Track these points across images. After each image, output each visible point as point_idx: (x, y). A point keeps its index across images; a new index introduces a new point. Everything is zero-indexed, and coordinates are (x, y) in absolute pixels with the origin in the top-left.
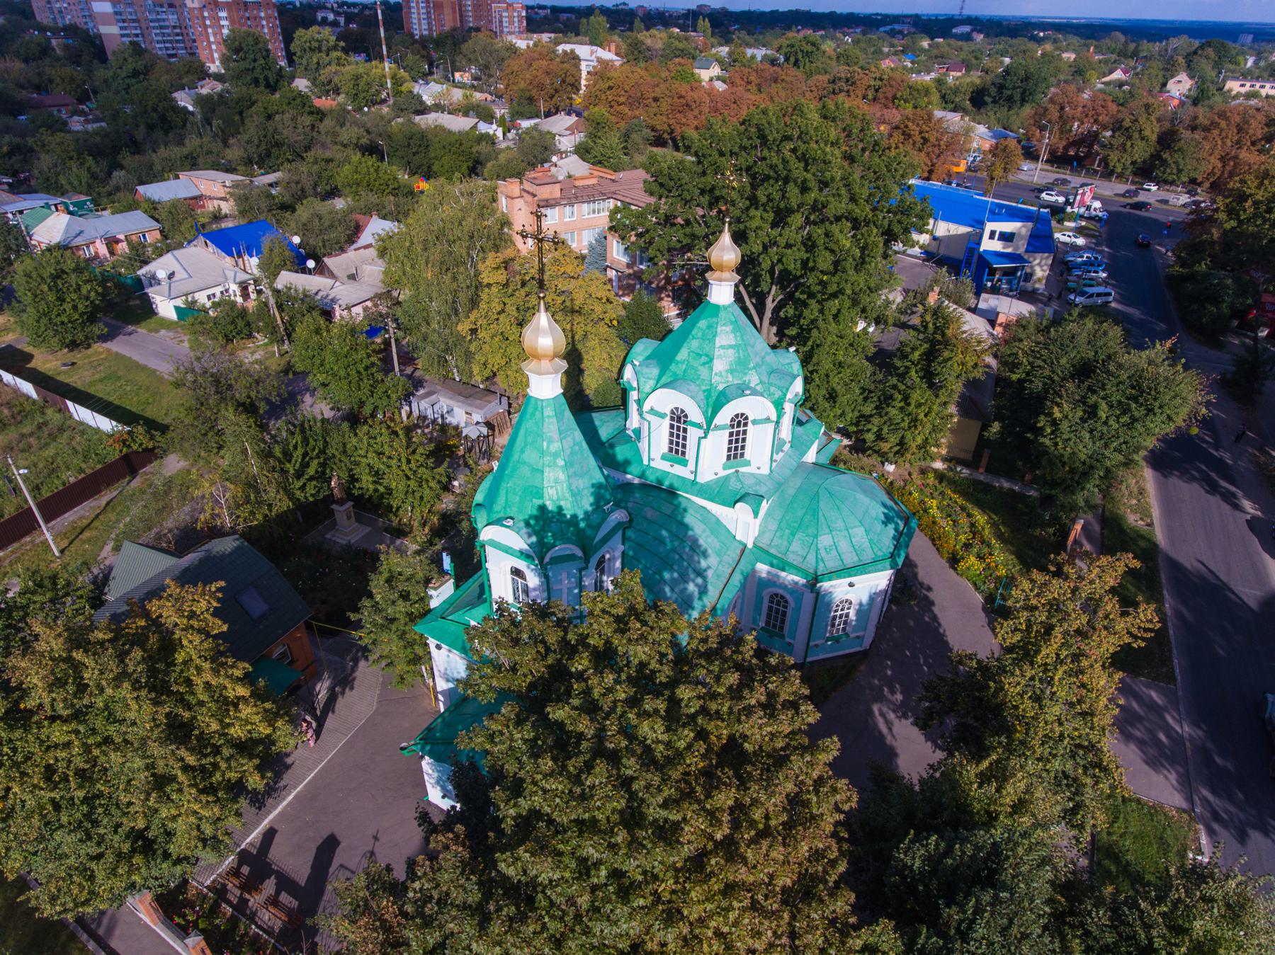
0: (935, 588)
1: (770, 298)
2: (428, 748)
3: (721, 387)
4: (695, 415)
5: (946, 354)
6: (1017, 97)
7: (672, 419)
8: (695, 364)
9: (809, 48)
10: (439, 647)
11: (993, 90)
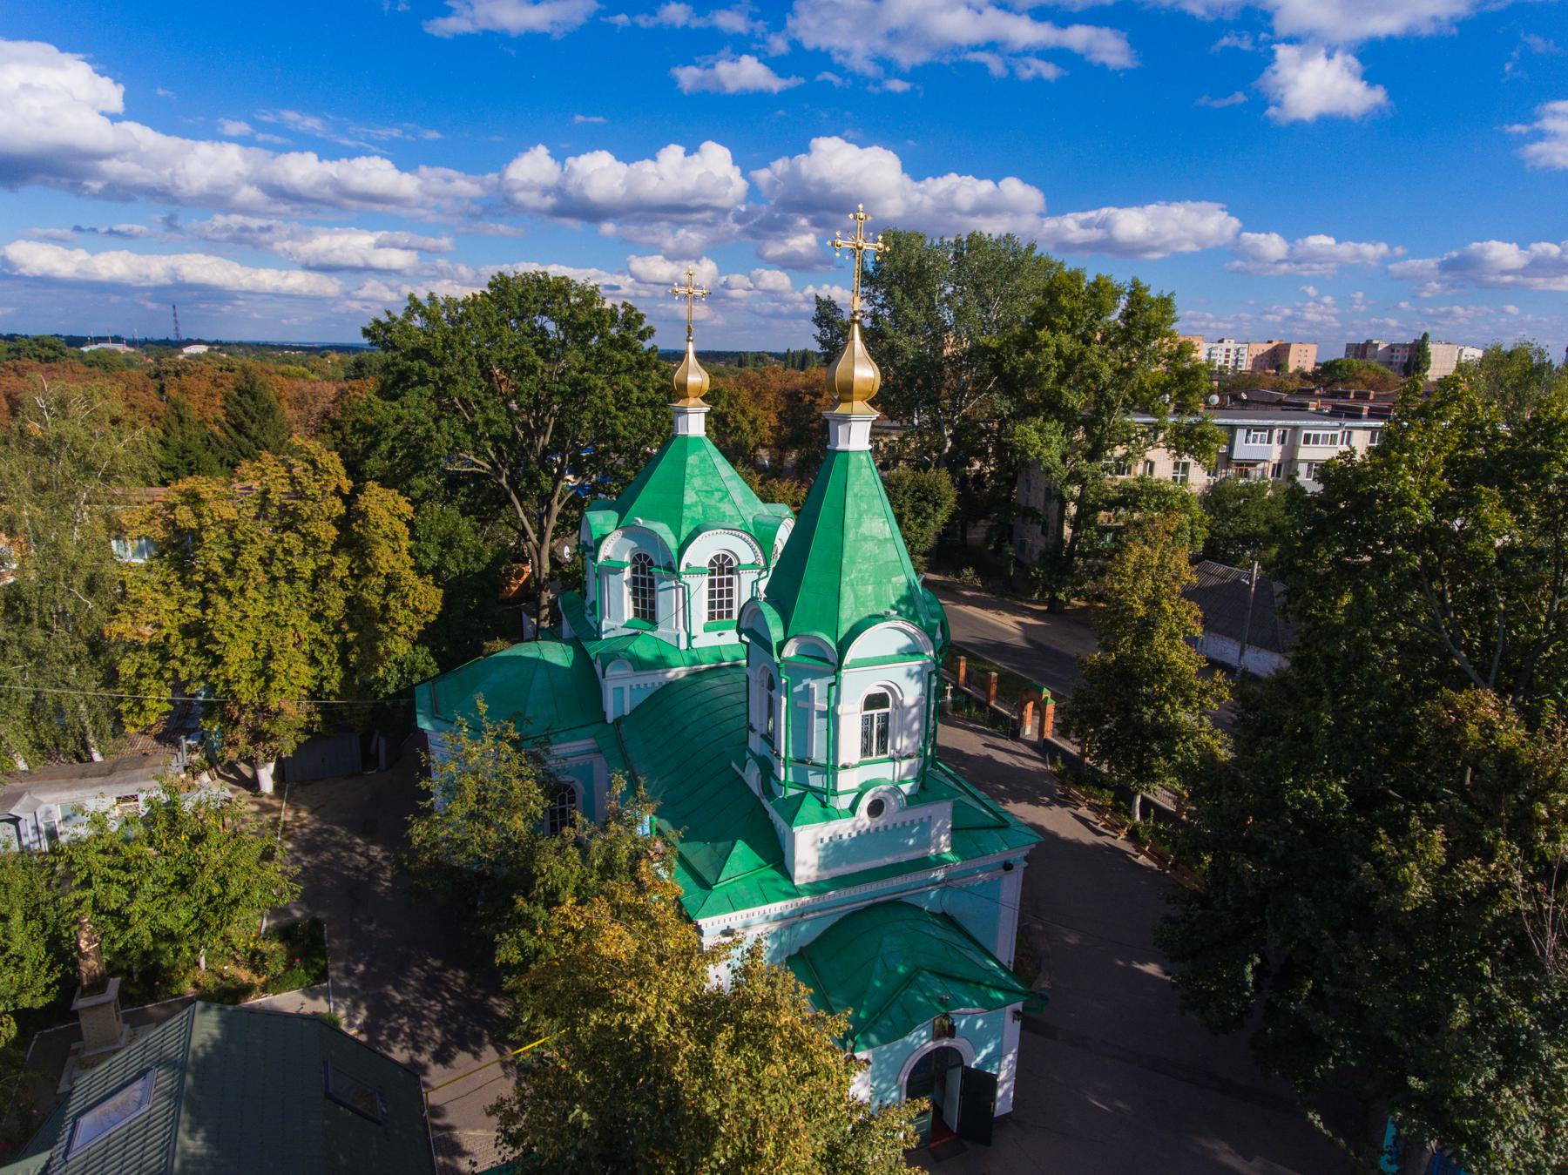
1: (556, 498)
2: (873, 1038)
3: (751, 520)
4: (746, 553)
7: (713, 573)
8: (712, 502)
9: (51, 353)
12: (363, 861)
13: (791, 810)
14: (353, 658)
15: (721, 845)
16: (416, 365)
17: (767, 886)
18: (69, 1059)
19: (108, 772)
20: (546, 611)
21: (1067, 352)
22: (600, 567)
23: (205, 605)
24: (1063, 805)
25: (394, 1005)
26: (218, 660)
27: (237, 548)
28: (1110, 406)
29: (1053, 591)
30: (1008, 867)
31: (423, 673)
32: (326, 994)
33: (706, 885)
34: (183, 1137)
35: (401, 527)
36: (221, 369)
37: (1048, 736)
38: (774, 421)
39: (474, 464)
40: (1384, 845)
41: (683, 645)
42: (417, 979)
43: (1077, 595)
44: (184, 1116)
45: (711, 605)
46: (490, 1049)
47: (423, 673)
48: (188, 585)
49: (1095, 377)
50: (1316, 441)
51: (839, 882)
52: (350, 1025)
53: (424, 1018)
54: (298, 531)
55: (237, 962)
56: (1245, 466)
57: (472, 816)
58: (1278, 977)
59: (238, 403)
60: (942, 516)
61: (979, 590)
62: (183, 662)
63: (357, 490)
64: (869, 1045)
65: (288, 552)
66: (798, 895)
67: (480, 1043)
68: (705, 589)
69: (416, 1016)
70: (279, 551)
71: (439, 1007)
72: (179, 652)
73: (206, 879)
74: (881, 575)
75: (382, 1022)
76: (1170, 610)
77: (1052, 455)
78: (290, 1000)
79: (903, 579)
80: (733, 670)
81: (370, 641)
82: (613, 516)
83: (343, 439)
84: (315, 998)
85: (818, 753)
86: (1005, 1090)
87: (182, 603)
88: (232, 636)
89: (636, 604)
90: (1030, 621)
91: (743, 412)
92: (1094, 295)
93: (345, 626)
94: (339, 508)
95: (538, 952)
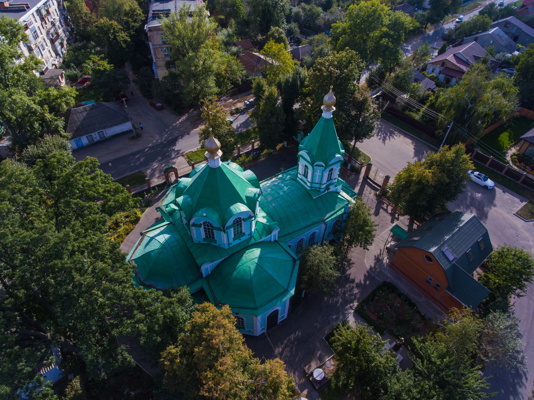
0: (155, 217)
15: (338, 201)
25: (343, 301)
42: (333, 300)
52: (354, 305)
53: (344, 291)
67: (347, 276)
69: (344, 293)
75: (349, 300)
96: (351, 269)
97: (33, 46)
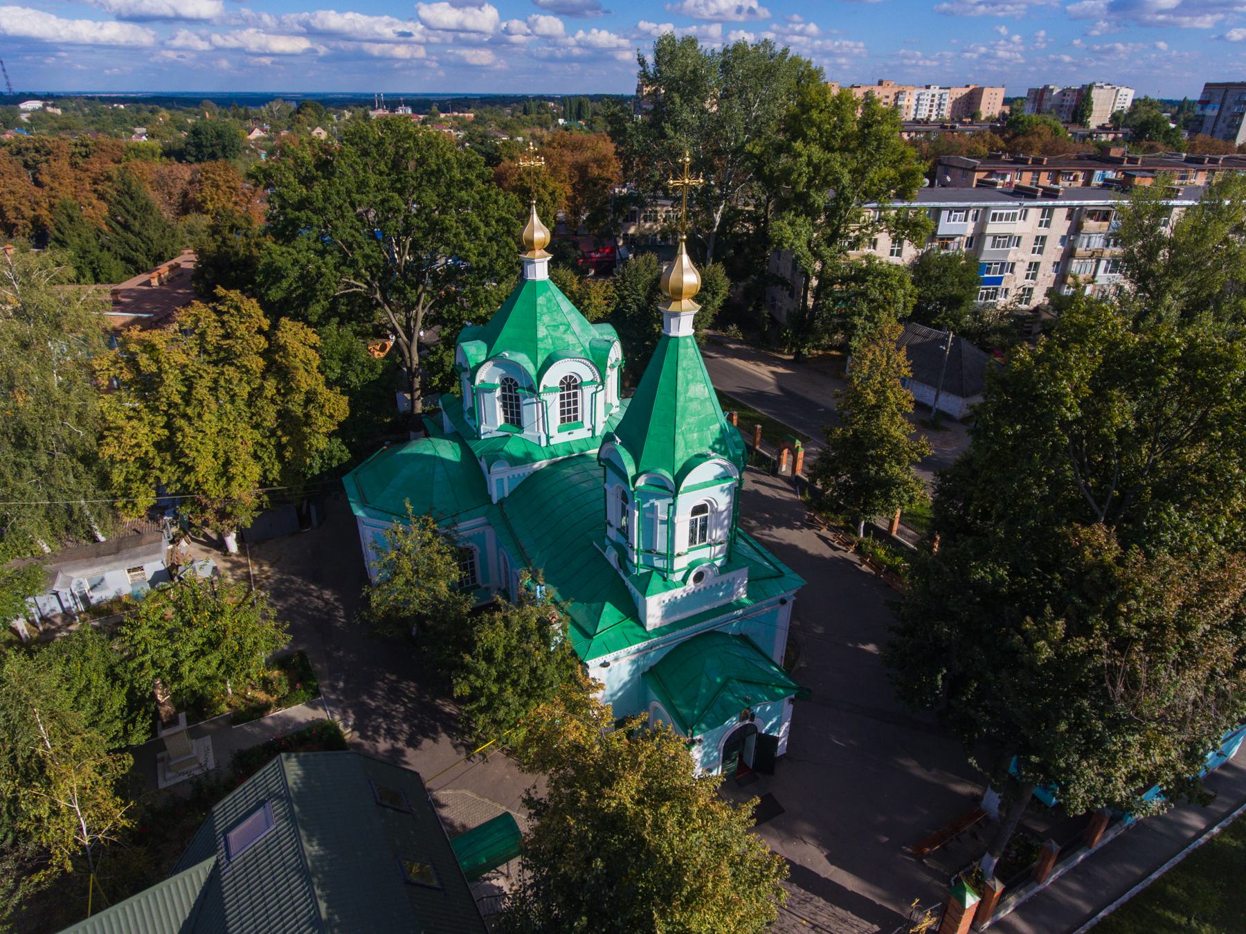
2: (703, 726)
4: (586, 372)
5: (586, 302)
6: (220, 154)
7: (563, 389)
8: (558, 334)
10: (605, 665)
11: (193, 150)
12: (320, 604)
13: (644, 584)
14: (287, 454)
15: (594, 605)
16: (303, 215)
17: (627, 631)
18: (160, 765)
19: (117, 549)
20: (419, 392)
21: (815, 161)
22: (478, 389)
23: (168, 426)
24: (810, 527)
26: (189, 470)
27: (189, 383)
28: (847, 201)
29: (799, 347)
30: (783, 602)
31: (340, 459)
32: (322, 704)
33: (589, 636)
34: (306, 845)
35: (312, 354)
36: (76, 145)
37: (799, 473)
38: (570, 192)
39: (353, 286)
40: (1029, 624)
41: (544, 443)
42: (382, 690)
43: (816, 347)
44: (302, 832)
45: (562, 413)
46: (444, 738)
47: (340, 459)
48: (154, 410)
49: (837, 181)
50: (1001, 219)
51: (674, 626)
53: (394, 717)
54: (231, 364)
55: (253, 688)
56: (946, 241)
57: (407, 582)
58: (956, 684)
59: (119, 203)
60: (718, 302)
61: (741, 342)
62: (162, 470)
63: (275, 326)
64: (702, 731)
65: (229, 381)
66: (649, 638)
67: (436, 732)
68: (558, 402)
69: (387, 716)
70: (222, 382)
71: (402, 709)
72: (157, 463)
73: (230, 641)
74: (703, 425)
76: (892, 399)
77: (801, 246)
78: (300, 712)
79: (716, 427)
80: (581, 460)
81: (299, 442)
82: (483, 347)
83: (224, 242)
84: (315, 708)
85: (661, 546)
86: (783, 742)
87: (152, 425)
88: (198, 451)
89: (506, 413)
90: (780, 370)
91: (544, 186)
92: (837, 107)
93: (279, 433)
94: (263, 343)
95: (482, 688)
96: (450, 747)
97: (1080, 251)
